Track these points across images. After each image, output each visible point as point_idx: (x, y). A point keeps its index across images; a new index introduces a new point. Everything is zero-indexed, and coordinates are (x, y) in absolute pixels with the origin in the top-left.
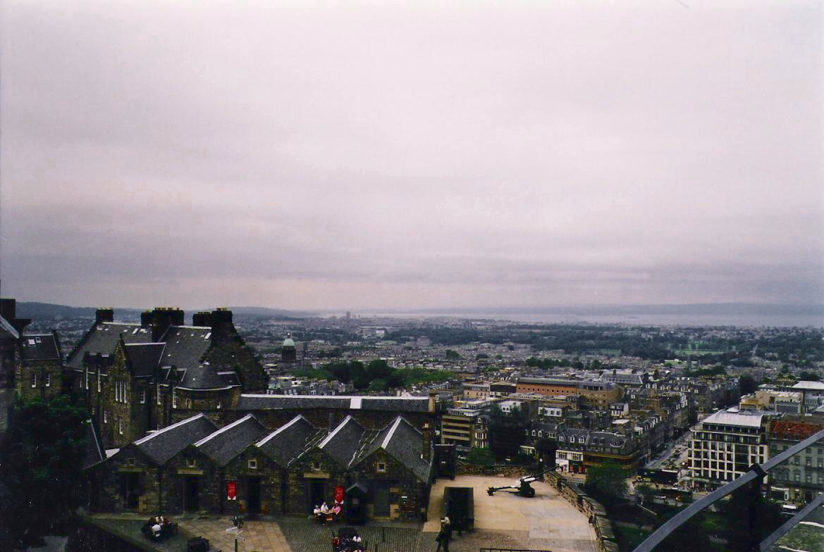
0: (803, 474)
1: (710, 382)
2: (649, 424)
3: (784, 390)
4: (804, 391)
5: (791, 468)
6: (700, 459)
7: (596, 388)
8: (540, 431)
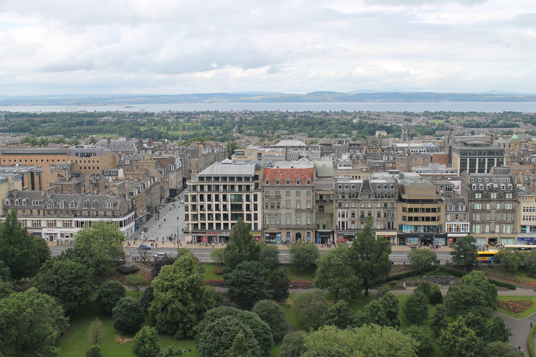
0: (293, 217)
1: (201, 146)
2: (144, 185)
3: (268, 147)
4: (287, 148)
5: (283, 212)
6: (196, 213)
7: (89, 155)
8: (24, 200)
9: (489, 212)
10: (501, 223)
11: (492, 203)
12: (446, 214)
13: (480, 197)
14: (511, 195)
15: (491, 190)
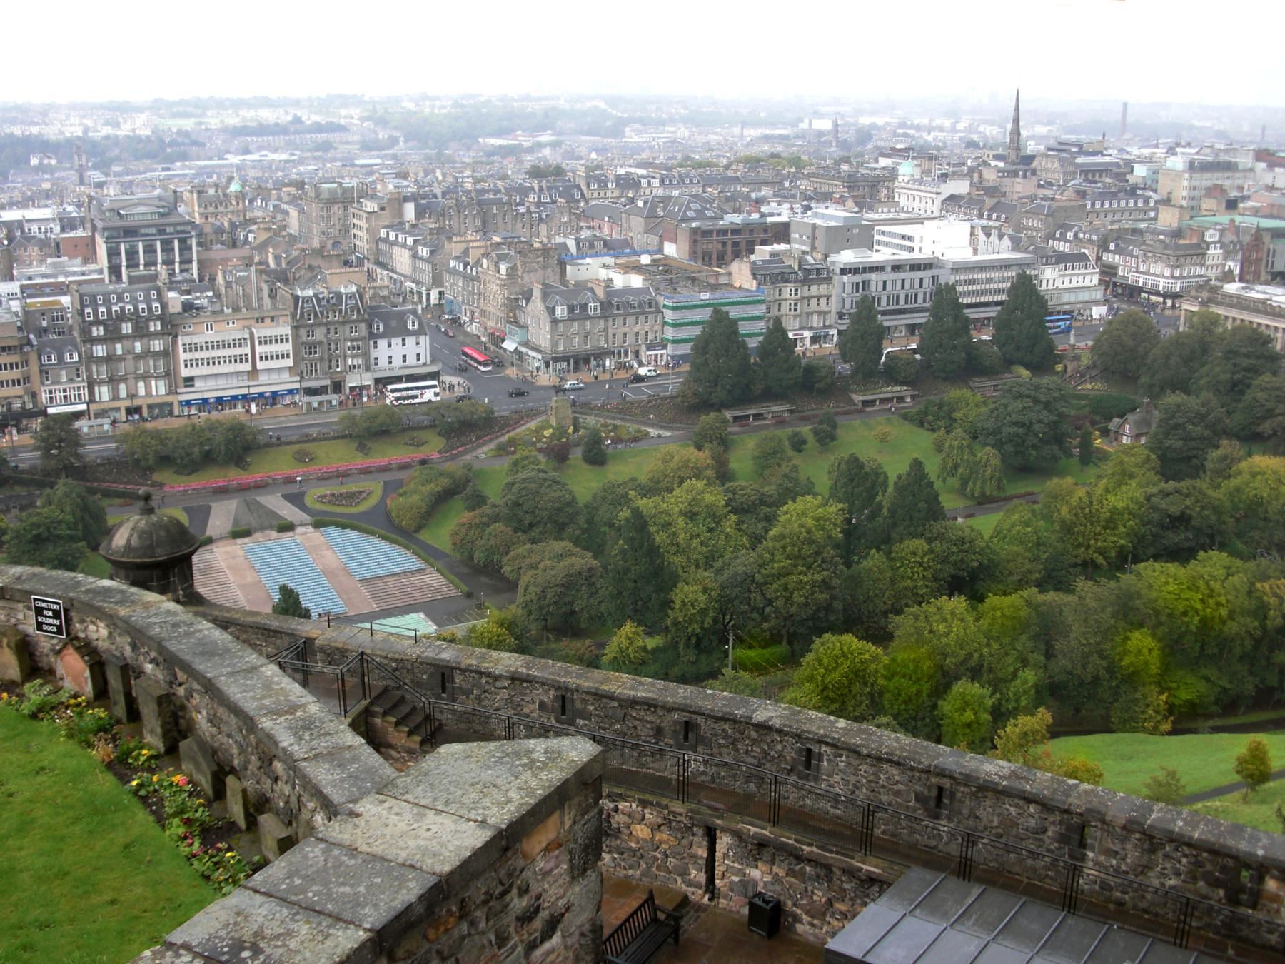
9: (121, 359)
10: (146, 377)
11: (125, 342)
12: (41, 371)
13: (102, 333)
14: (159, 323)
15: (122, 317)
